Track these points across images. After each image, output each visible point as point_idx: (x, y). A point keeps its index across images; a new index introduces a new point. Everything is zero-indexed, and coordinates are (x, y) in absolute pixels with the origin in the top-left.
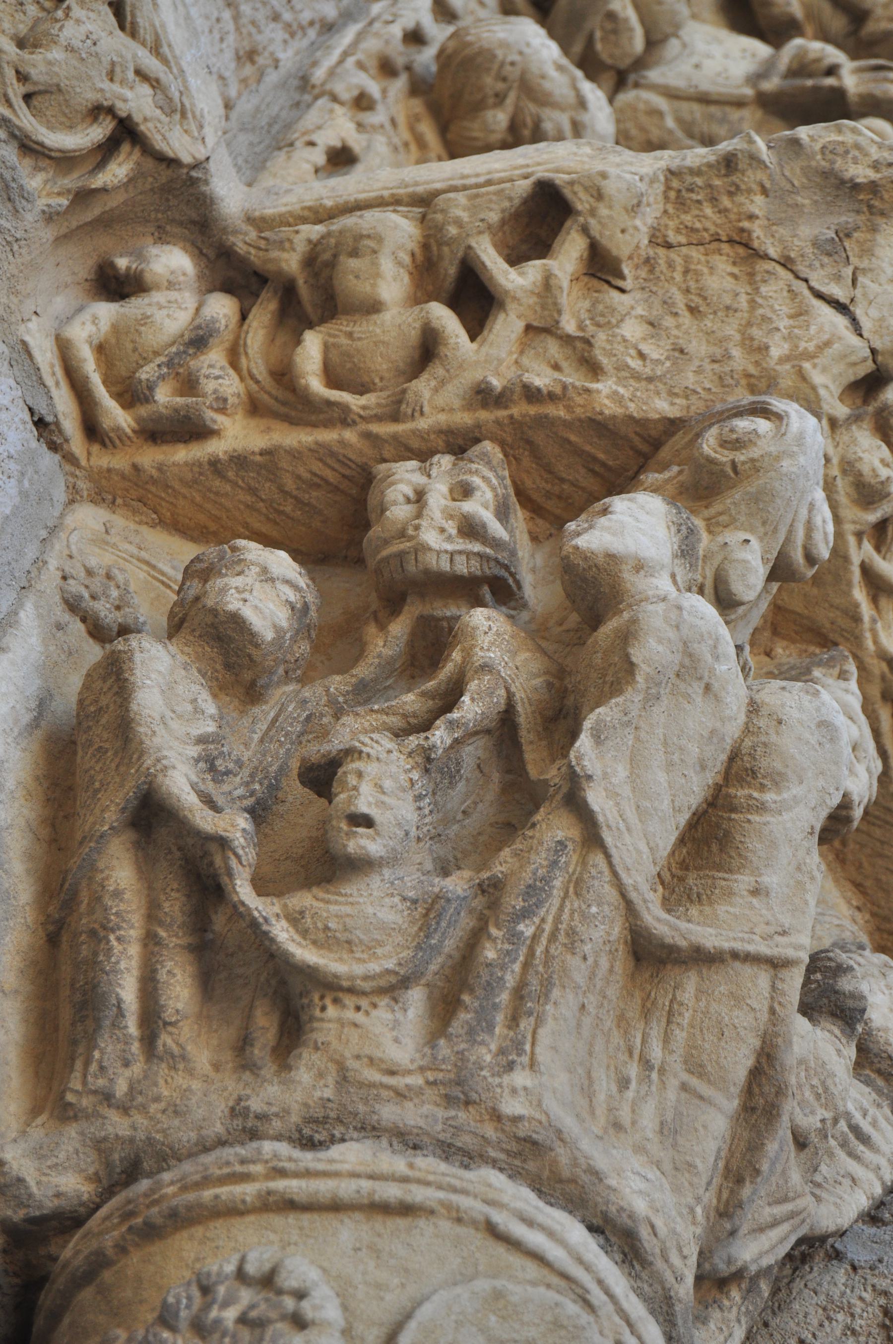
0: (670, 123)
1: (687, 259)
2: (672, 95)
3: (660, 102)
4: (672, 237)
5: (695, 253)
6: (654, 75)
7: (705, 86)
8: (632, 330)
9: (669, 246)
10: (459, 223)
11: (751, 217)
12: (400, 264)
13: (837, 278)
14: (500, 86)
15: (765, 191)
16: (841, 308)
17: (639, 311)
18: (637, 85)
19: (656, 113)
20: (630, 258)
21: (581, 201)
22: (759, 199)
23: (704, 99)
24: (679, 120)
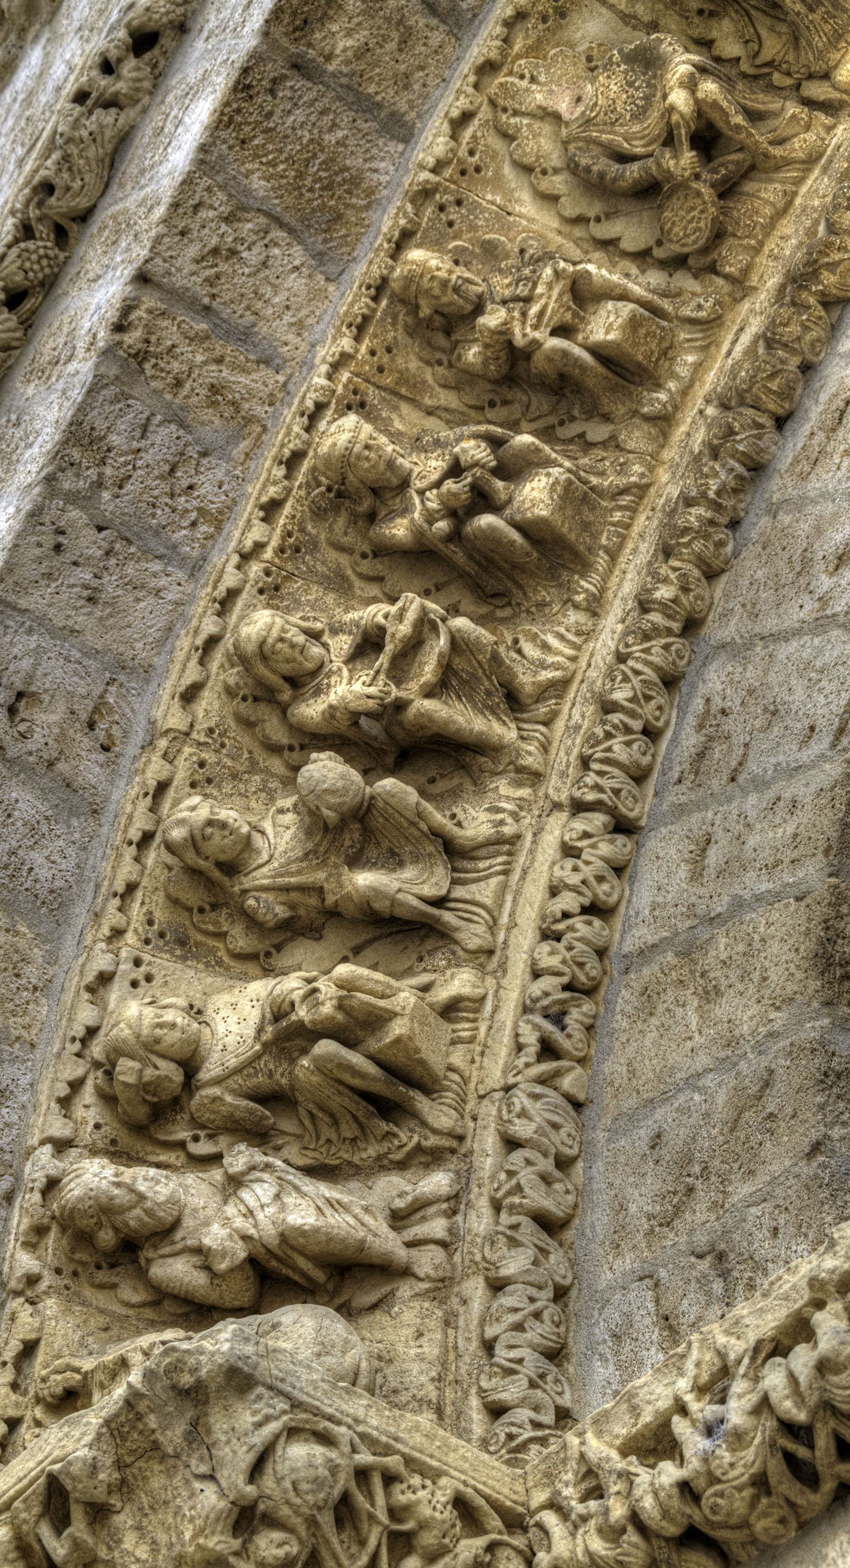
0: (229, 1098)
1: (140, 1469)
2: (218, 1081)
3: (215, 1091)
4: (128, 1460)
5: (141, 1463)
6: (204, 1075)
7: (232, 1062)
8: (129, 1541)
9: (128, 1466)
10: (25, 1521)
11: (153, 1431)
12: (13, 1561)
13: (201, 1459)
14: (94, 1220)
15: (152, 1411)
16: (211, 1477)
17: (130, 1522)
18: (198, 1088)
19: (215, 1099)
20: (109, 1493)
21: (68, 1484)
22: (152, 1417)
23: (237, 1071)
24: (233, 1092)
